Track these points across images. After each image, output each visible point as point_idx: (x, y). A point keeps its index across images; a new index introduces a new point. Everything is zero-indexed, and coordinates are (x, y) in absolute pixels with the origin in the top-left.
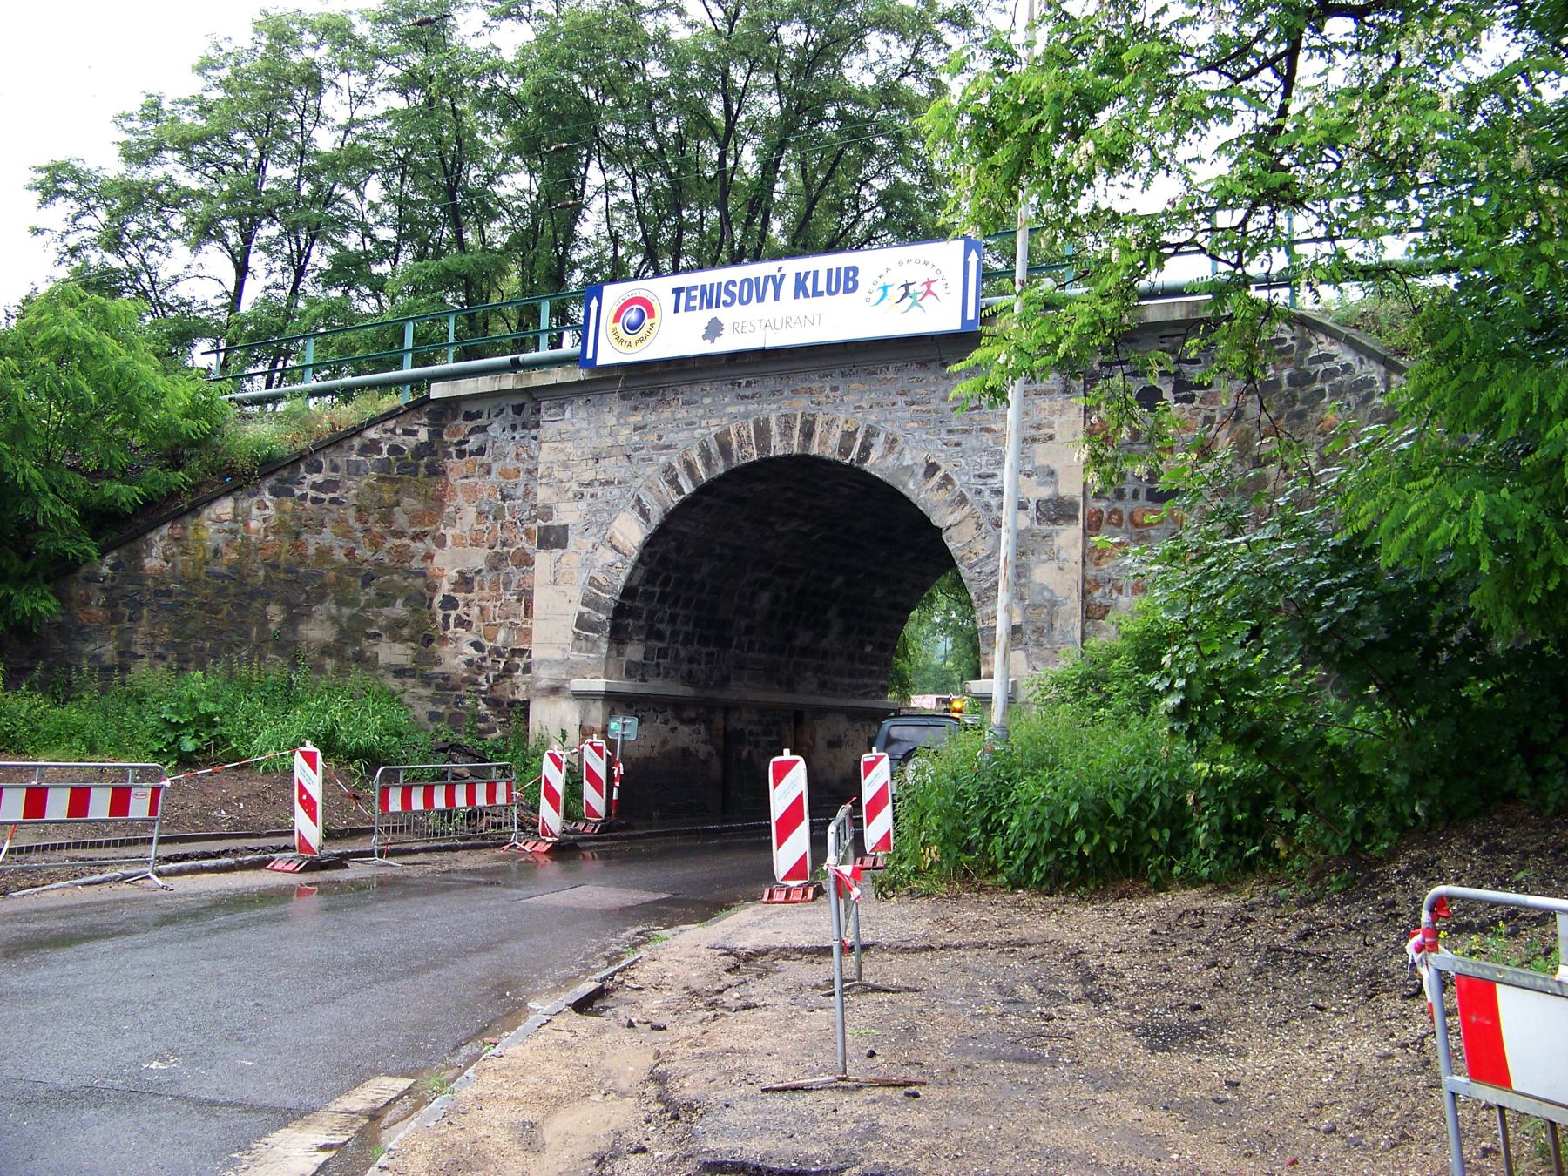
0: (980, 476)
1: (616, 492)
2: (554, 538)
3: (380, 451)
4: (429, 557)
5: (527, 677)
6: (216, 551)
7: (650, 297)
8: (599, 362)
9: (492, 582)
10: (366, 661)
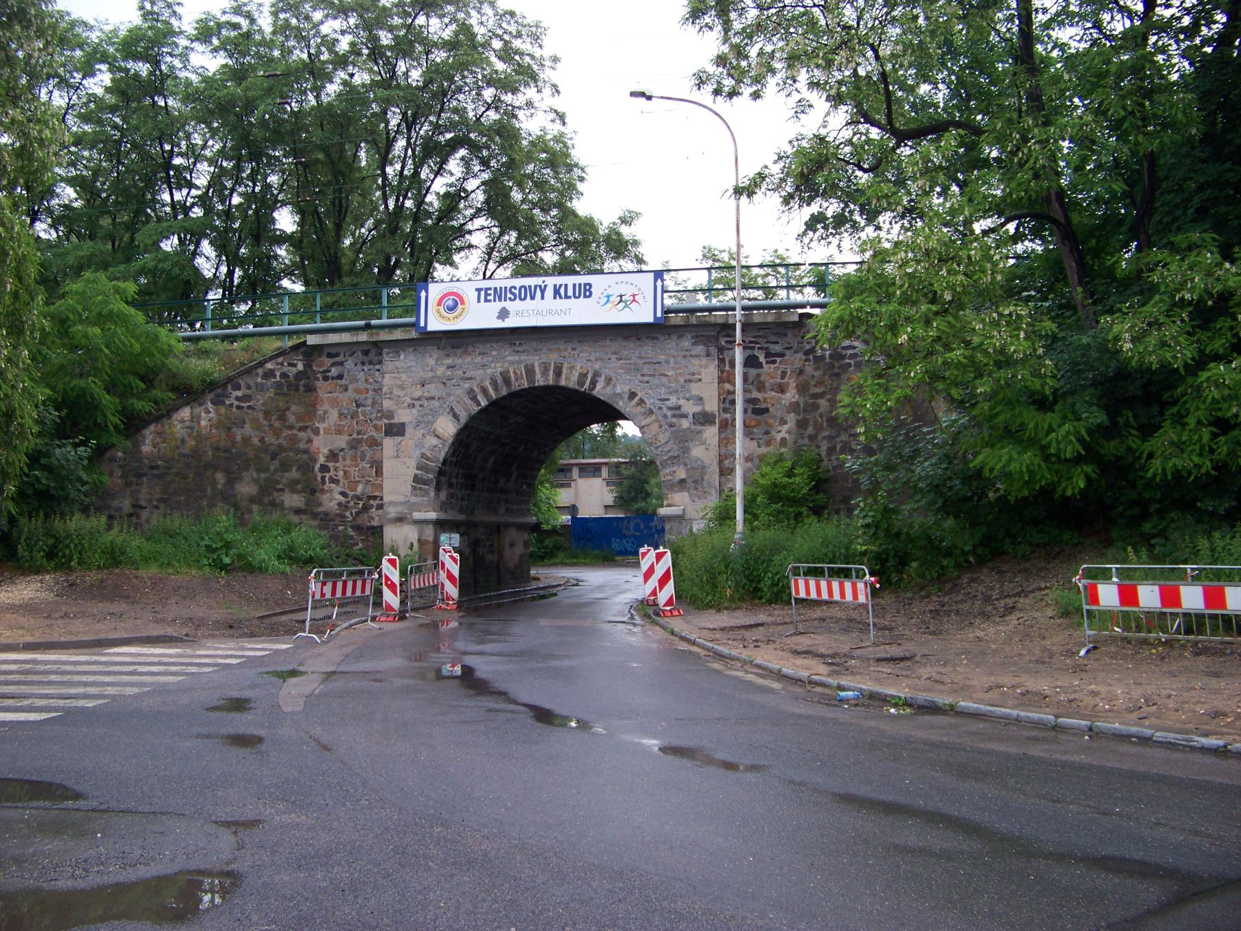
0: (661, 400)
1: (436, 404)
2: (396, 430)
3: (275, 377)
4: (310, 441)
5: (380, 512)
6: (183, 440)
7: (460, 292)
8: (430, 329)
9: (352, 456)
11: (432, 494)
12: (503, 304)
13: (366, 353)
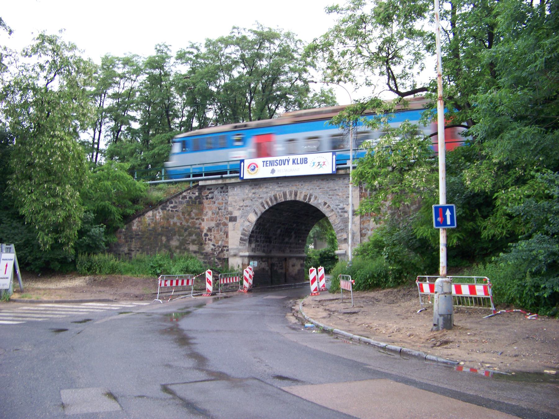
1: (248, 208)
2: (233, 219)
4: (200, 224)
5: (227, 252)
6: (149, 224)
8: (245, 178)
10: (187, 250)
11: (247, 245)
12: (273, 167)
13: (222, 188)
